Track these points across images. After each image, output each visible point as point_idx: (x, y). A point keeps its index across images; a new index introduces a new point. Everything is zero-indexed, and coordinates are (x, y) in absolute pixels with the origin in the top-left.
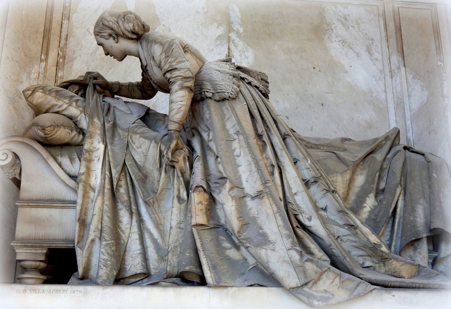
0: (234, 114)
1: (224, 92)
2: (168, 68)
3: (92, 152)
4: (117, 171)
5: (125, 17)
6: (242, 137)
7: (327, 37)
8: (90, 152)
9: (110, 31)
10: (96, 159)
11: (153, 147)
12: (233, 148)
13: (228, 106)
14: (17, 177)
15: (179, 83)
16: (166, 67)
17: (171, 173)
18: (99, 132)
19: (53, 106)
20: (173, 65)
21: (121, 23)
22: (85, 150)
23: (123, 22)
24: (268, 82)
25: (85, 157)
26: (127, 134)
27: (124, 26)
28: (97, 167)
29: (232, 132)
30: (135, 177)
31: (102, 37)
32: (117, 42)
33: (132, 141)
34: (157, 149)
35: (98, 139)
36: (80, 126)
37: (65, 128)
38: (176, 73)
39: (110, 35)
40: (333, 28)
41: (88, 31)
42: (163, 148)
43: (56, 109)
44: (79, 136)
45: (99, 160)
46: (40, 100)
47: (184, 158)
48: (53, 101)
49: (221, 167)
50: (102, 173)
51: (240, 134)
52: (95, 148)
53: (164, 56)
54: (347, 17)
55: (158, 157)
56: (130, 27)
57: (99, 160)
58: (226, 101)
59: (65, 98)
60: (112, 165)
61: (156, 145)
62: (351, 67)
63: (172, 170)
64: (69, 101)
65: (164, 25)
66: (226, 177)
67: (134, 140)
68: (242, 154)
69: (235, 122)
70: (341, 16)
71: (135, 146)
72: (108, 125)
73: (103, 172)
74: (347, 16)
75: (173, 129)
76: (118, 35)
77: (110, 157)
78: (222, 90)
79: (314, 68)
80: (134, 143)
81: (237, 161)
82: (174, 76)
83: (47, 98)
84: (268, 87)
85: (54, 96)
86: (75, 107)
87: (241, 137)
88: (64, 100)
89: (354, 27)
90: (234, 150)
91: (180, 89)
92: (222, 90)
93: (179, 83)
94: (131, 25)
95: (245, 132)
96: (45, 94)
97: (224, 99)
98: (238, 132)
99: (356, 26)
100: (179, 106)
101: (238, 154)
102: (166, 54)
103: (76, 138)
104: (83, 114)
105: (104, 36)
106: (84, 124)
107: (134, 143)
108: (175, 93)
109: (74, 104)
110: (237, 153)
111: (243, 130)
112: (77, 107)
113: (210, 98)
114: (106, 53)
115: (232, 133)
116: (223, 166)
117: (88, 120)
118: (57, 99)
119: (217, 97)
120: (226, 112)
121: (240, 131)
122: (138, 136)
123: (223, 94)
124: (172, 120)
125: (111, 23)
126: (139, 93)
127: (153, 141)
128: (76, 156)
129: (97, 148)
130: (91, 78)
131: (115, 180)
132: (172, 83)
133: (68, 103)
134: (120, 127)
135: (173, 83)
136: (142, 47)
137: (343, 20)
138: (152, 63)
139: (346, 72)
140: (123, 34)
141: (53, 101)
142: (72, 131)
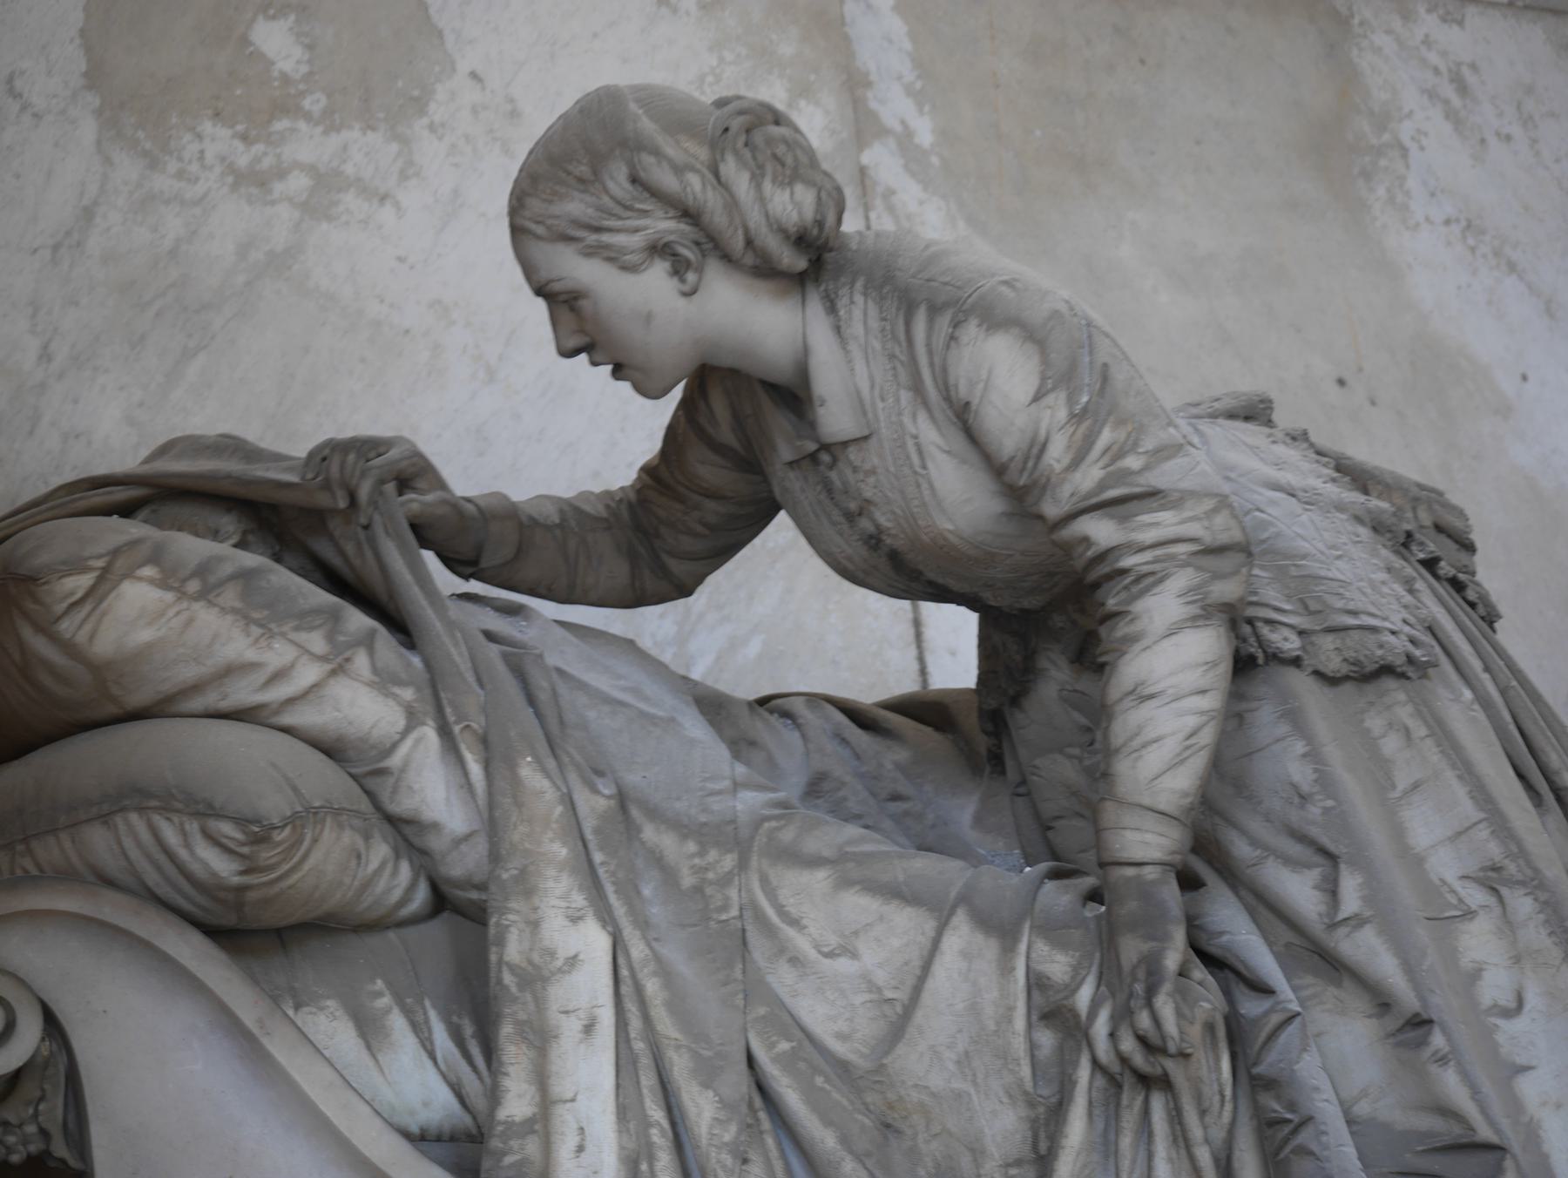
0: (1454, 767)
1: (1374, 630)
2: (1102, 486)
3: (545, 980)
4: (724, 1104)
5: (758, 137)
6: (1529, 901)
7: (1381, 191)
8: (535, 979)
9: (670, 225)
10: (570, 1028)
11: (966, 955)
12: (1466, 962)
13: (1405, 713)
14: (60, 1150)
15: (1181, 580)
16: (1088, 477)
17: (1129, 1120)
18: (561, 851)
19: (231, 671)
20: (1128, 473)
21: (742, 183)
22: (513, 969)
23: (757, 179)
24: (1470, 548)
25: (522, 1016)
26: (729, 861)
27: (762, 200)
28: (588, 1076)
29: (1446, 866)
30: (844, 1140)
31: (591, 252)
32: (689, 294)
33: (781, 910)
34: (1006, 970)
35: (565, 897)
36: (402, 805)
37: (341, 826)
38: (1160, 524)
39: (659, 249)
40: (1407, 142)
41: (14, 94)
42: (1057, 965)
43: (242, 693)
44: (395, 872)
45: (589, 1028)
46: (145, 635)
47: (1210, 1028)
48: (237, 645)
49: (1451, 1085)
50: (622, 1113)
51: (1512, 883)
52: (551, 953)
53: (1062, 414)
54: (1470, 78)
55: (1020, 1023)
56: (798, 205)
57: (589, 1028)
58: (1389, 683)
59: (306, 618)
60: (680, 1066)
61: (989, 948)
62: (1525, 378)
63: (1140, 1099)
64: (330, 638)
65: (474, 75)
66: (1494, 1139)
67: (785, 896)
68: (1533, 1000)
69: (1468, 809)
70: (1437, 71)
71: (802, 944)
72: (602, 804)
73: (625, 1111)
74: (1466, 71)
75: (1156, 854)
76: (713, 245)
77: (660, 1014)
78: (1354, 613)
79: (1341, 382)
80: (795, 922)
81: (1500, 1038)
82: (1149, 536)
83: (189, 622)
84: (1473, 574)
85: (234, 611)
86: (371, 684)
87: (1523, 904)
88: (302, 637)
89: (1508, 138)
90: (1476, 974)
91: (1195, 618)
92: (1354, 613)
93: (1181, 580)
94: (805, 197)
95: (1536, 870)
96: (182, 594)
97: (1386, 670)
98: (1496, 869)
99: (1516, 130)
100: (1192, 721)
101: (1507, 1000)
102: (1071, 401)
103: (382, 884)
104: (429, 733)
105: (622, 251)
106: (433, 789)
107: (795, 922)
108: (1166, 643)
109: (361, 661)
110: (1495, 986)
111: (1529, 863)
112: (384, 682)
113: (1296, 662)
114: (572, 343)
115: (1451, 875)
116: (1466, 1077)
117: (475, 769)
118: (256, 631)
119: (1329, 653)
120: (1391, 745)
121: (1512, 868)
122: (820, 879)
123: (1371, 639)
124: (1146, 801)
125: (694, 181)
126: (616, 571)
127: (961, 920)
128: (386, 1001)
129: (563, 954)
130: (382, 482)
131: (728, 1159)
132: (1138, 580)
133: (323, 659)
134: (654, 814)
135: (1146, 581)
136: (838, 329)
137: (1448, 91)
138: (930, 434)
139: (1504, 410)
140: (749, 243)
141: (237, 645)
142: (367, 837)
